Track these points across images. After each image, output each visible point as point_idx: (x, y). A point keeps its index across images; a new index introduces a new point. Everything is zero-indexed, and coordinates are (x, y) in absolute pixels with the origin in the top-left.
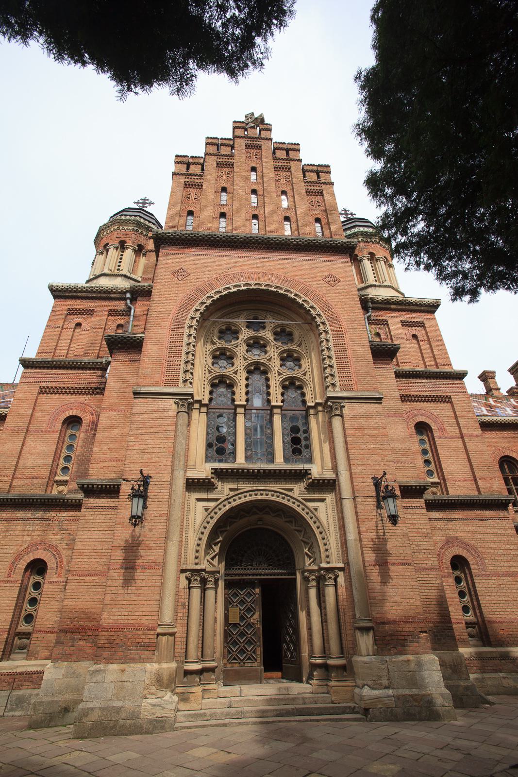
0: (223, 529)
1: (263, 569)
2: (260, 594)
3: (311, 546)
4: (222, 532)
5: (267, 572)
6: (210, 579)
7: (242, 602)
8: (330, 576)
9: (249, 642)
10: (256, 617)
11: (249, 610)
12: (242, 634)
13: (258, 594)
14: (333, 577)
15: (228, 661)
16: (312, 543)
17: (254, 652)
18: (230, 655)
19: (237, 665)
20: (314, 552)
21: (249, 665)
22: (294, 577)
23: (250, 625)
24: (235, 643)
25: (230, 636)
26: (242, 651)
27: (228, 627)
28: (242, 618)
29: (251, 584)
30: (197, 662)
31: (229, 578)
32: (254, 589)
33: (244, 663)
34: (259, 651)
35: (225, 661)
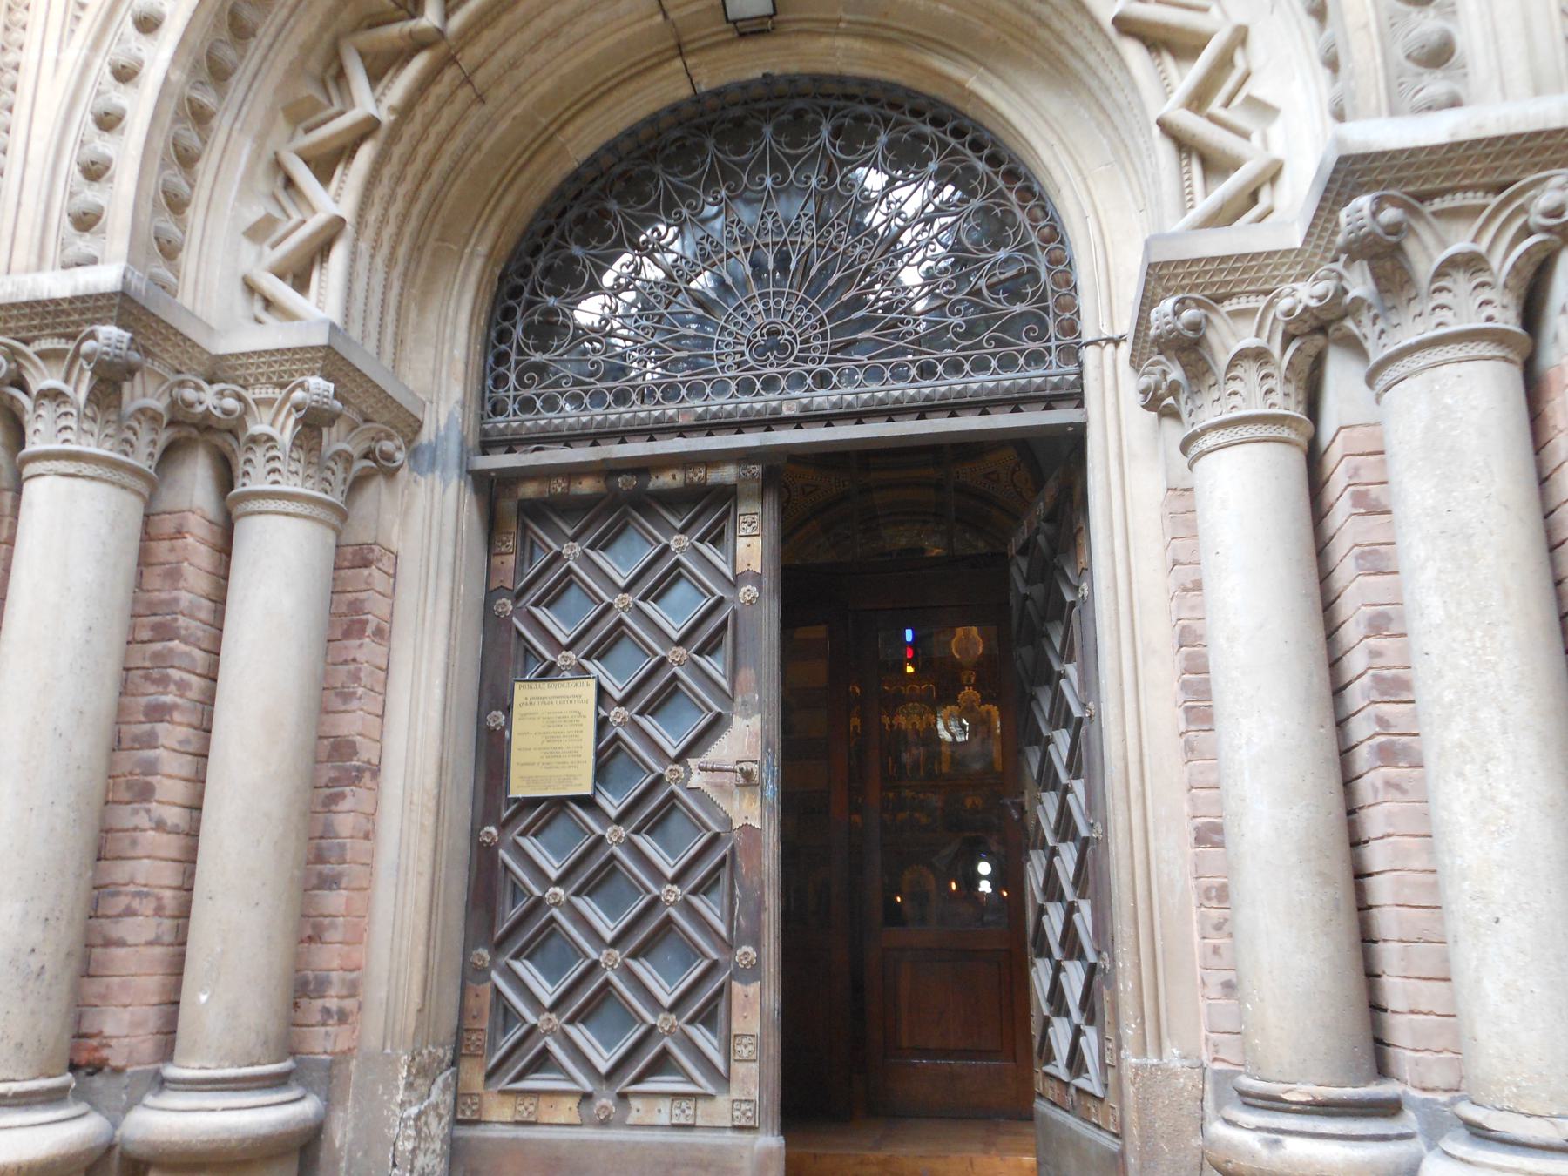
0: (394, 31)
1: (798, 381)
2: (767, 583)
3: (1224, 62)
4: (380, 68)
5: (822, 399)
6: (255, 428)
7: (606, 642)
8: (1461, 241)
9: (653, 936)
10: (747, 738)
11: (660, 695)
12: (597, 874)
13: (757, 579)
14: (1503, 262)
15: (490, 1075)
16: (1241, 37)
17: (707, 1017)
18: (516, 1033)
19: (567, 1110)
20: (1264, 110)
21: (663, 1113)
22: (1062, 416)
23: (658, 811)
24: (542, 941)
25: (518, 890)
26: (594, 1003)
27: (503, 826)
28: (609, 754)
29: (708, 506)
30: (52, 1097)
31: (500, 461)
32: (716, 537)
33: (623, 1096)
34: (755, 1008)
35: (474, 1075)
